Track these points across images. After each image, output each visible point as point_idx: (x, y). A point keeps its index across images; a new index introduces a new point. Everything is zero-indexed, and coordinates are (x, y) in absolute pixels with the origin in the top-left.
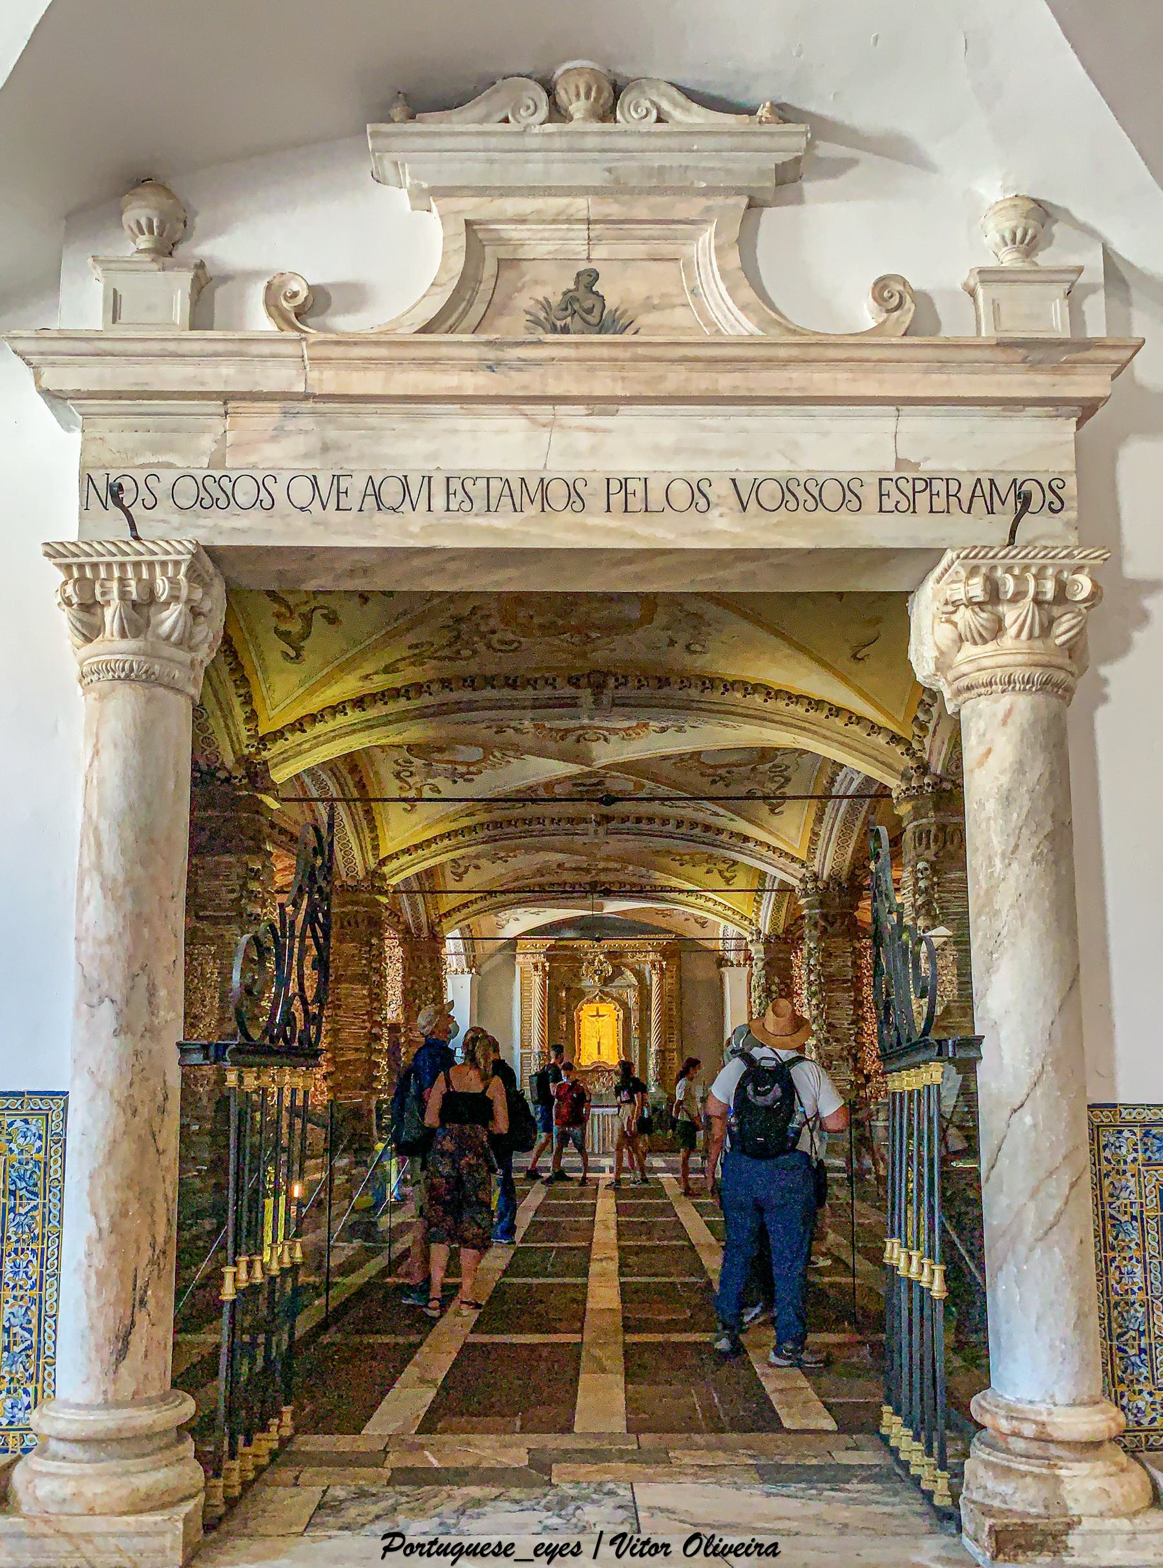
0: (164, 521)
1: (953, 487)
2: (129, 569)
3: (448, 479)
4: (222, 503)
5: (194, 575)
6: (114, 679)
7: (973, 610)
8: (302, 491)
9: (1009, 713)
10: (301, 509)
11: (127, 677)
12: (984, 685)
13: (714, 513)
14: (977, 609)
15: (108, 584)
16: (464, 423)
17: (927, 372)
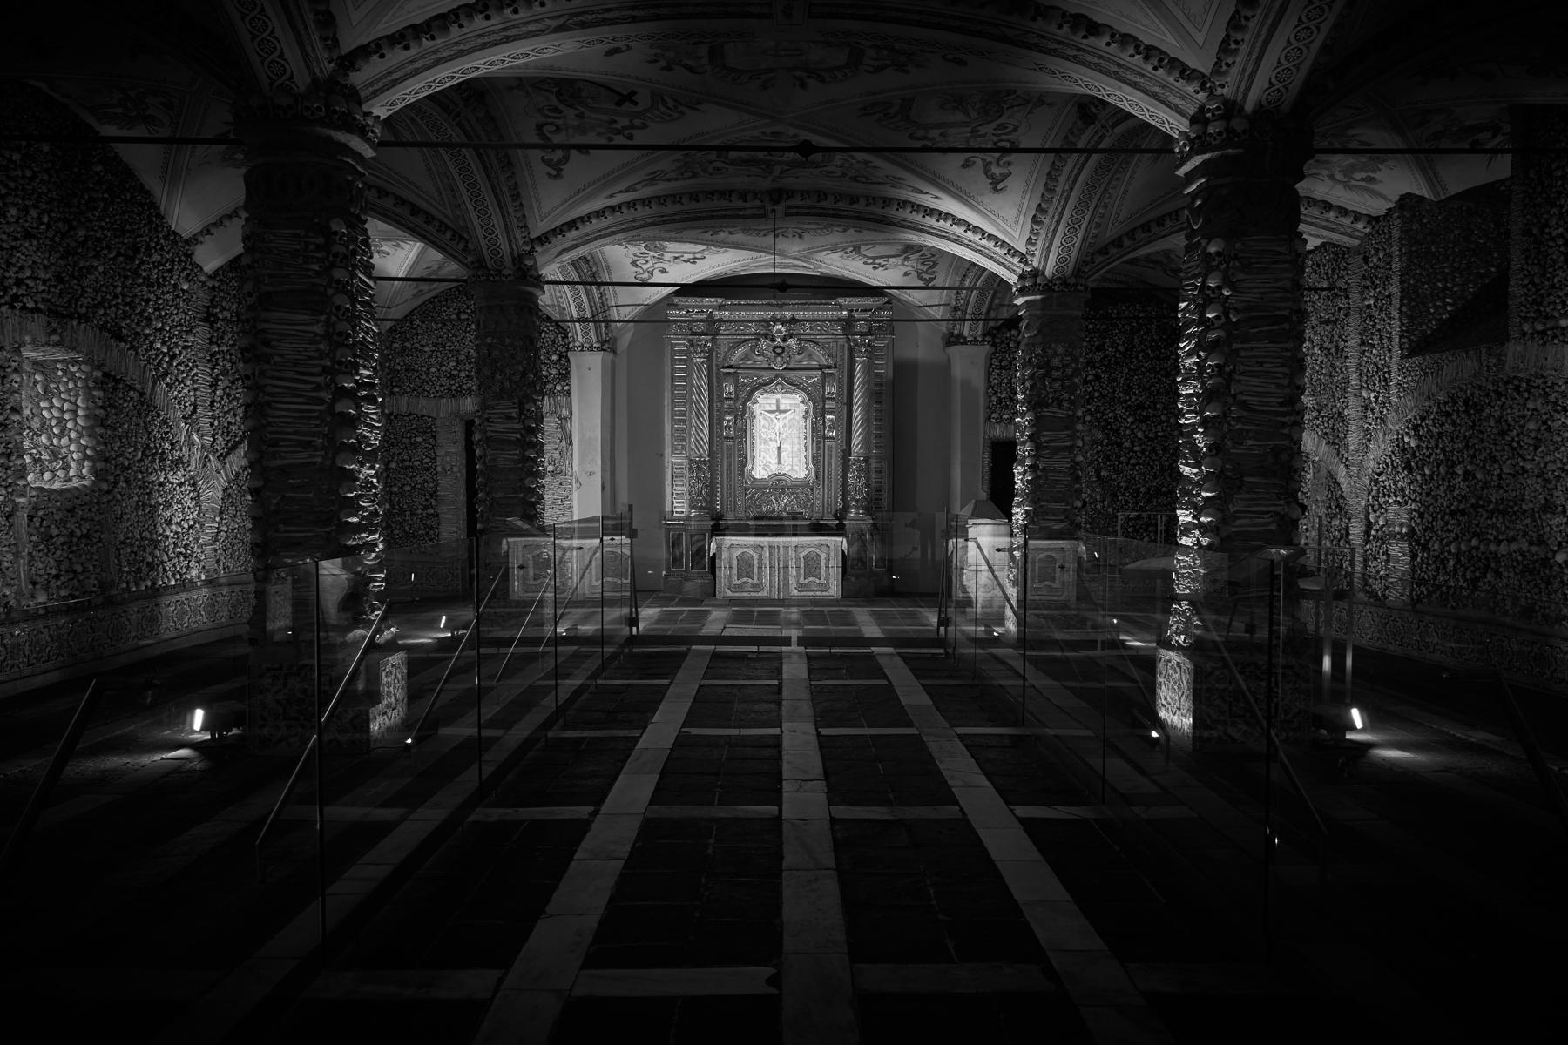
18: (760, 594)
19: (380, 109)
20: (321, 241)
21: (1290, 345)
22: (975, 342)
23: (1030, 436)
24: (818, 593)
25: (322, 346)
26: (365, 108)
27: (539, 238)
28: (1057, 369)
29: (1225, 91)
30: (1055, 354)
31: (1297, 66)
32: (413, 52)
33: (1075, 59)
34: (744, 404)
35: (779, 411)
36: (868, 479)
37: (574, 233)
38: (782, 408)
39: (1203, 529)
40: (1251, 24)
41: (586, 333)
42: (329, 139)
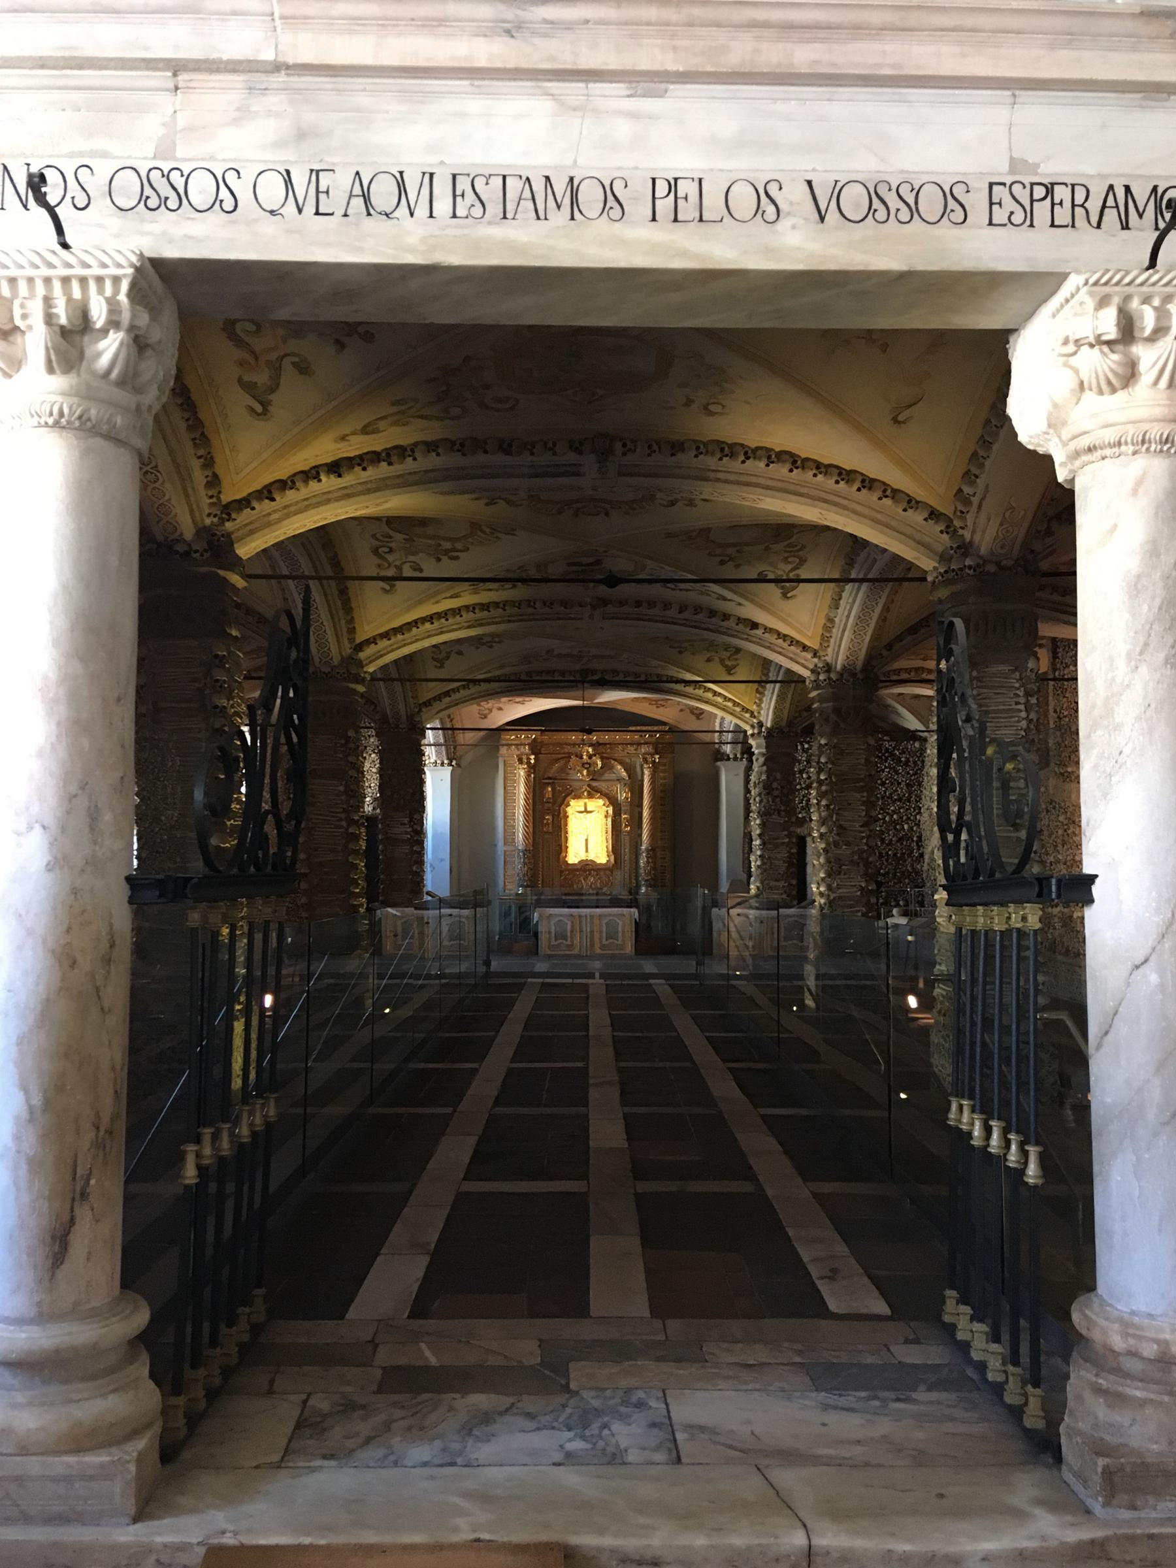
0: (100, 226)
1: (1079, 199)
2: (57, 285)
3: (454, 176)
4: (173, 203)
5: (137, 292)
6: (39, 426)
7: (1102, 352)
8: (272, 190)
9: (1139, 482)
10: (272, 212)
11: (56, 424)
12: (1111, 446)
13: (784, 224)
14: (1106, 349)
15: (29, 304)
16: (475, 105)
17: (1052, 46)
18: (572, 952)
19: (371, 669)
20: (343, 742)
21: (865, 794)
22: (735, 759)
23: (760, 835)
24: (616, 952)
25: (343, 798)
26: (365, 669)
27: (424, 703)
28: (777, 789)
29: (826, 658)
30: (776, 779)
31: (860, 650)
32: (393, 640)
33: (747, 640)
34: (560, 806)
35: (586, 811)
36: (655, 863)
37: (447, 699)
38: (589, 809)
39: (821, 894)
40: (834, 630)
41: (438, 753)
42: (348, 688)
